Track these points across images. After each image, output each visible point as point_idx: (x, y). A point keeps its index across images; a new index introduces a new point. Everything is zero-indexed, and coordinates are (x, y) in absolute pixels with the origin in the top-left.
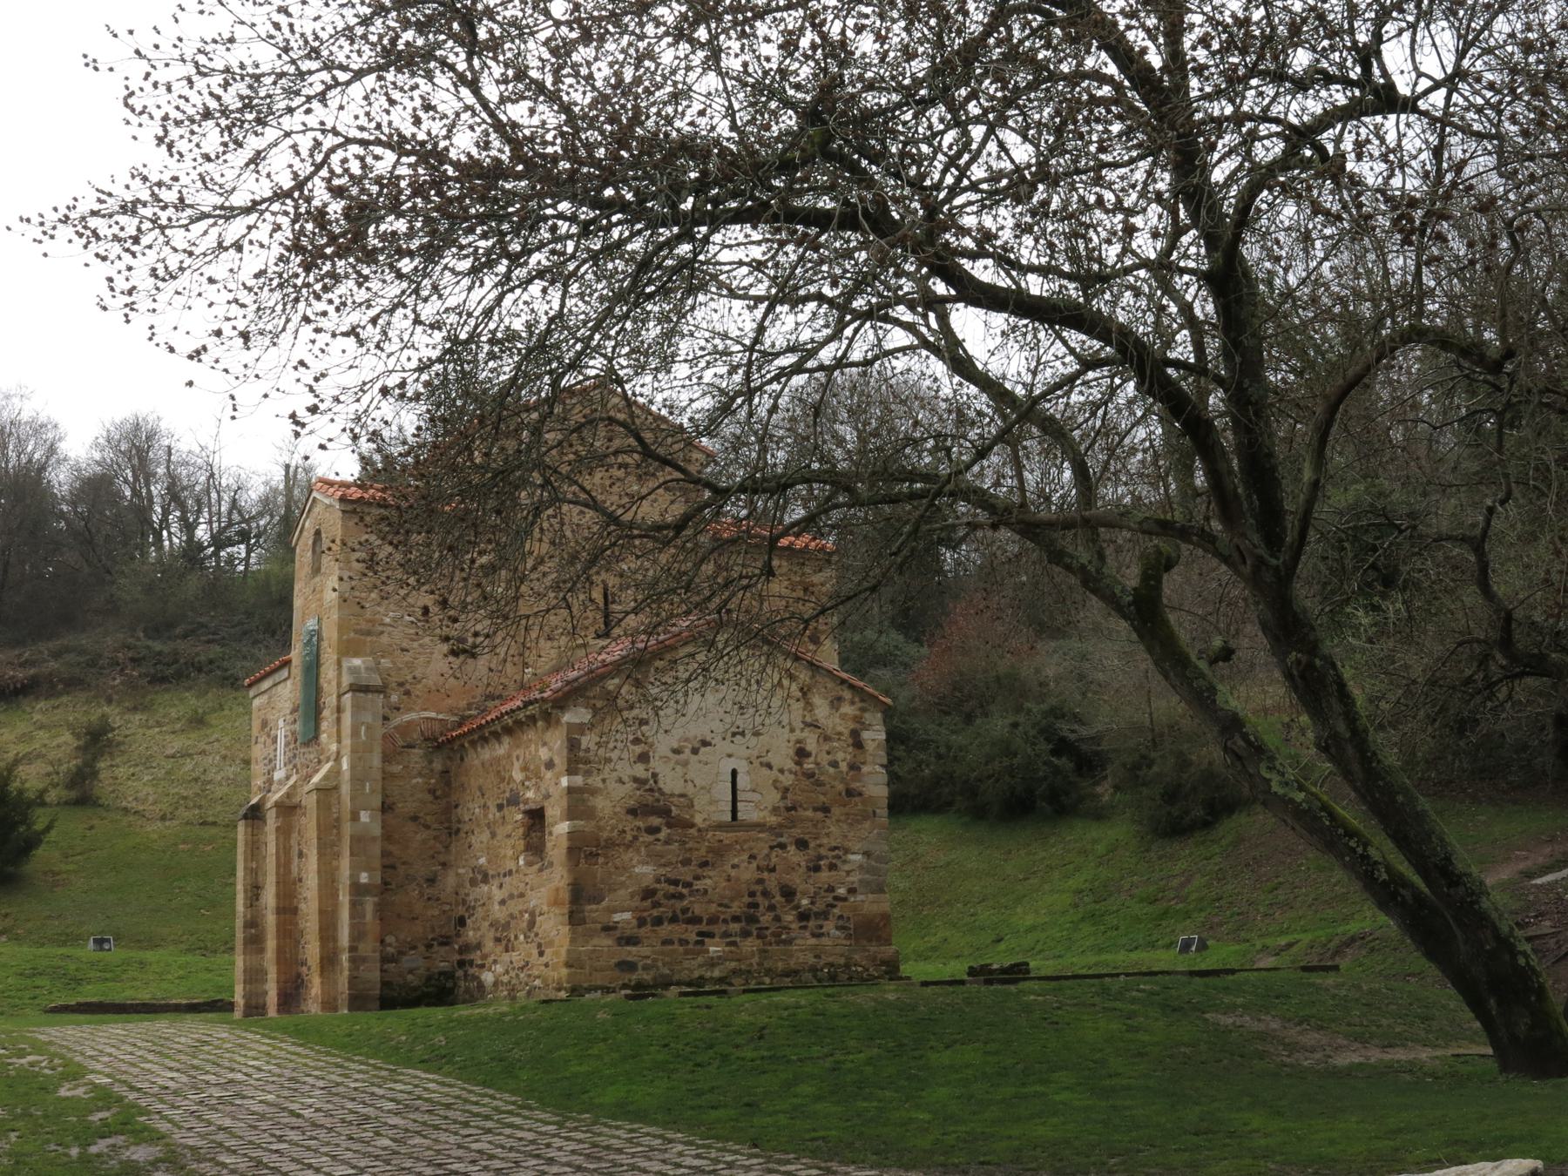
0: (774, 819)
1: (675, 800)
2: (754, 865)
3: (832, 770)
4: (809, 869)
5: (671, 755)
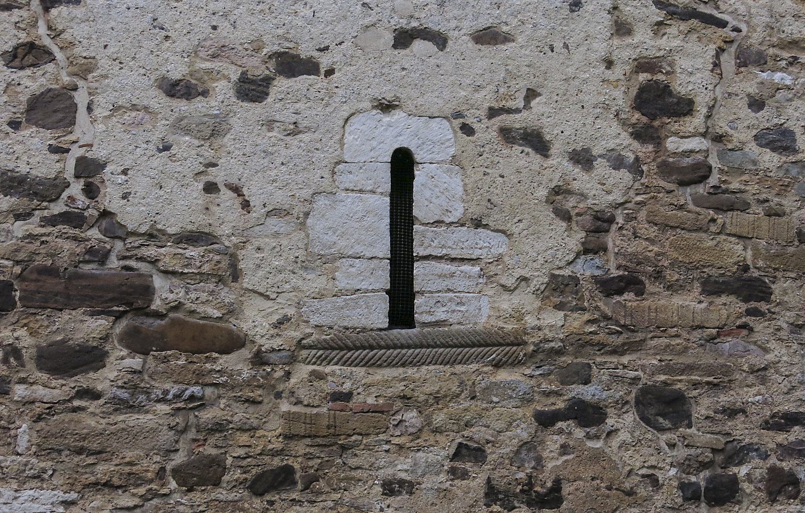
0: (553, 318)
1: (167, 254)
2: (477, 483)
3: (770, 159)
4: (691, 494)
5: (157, 100)
